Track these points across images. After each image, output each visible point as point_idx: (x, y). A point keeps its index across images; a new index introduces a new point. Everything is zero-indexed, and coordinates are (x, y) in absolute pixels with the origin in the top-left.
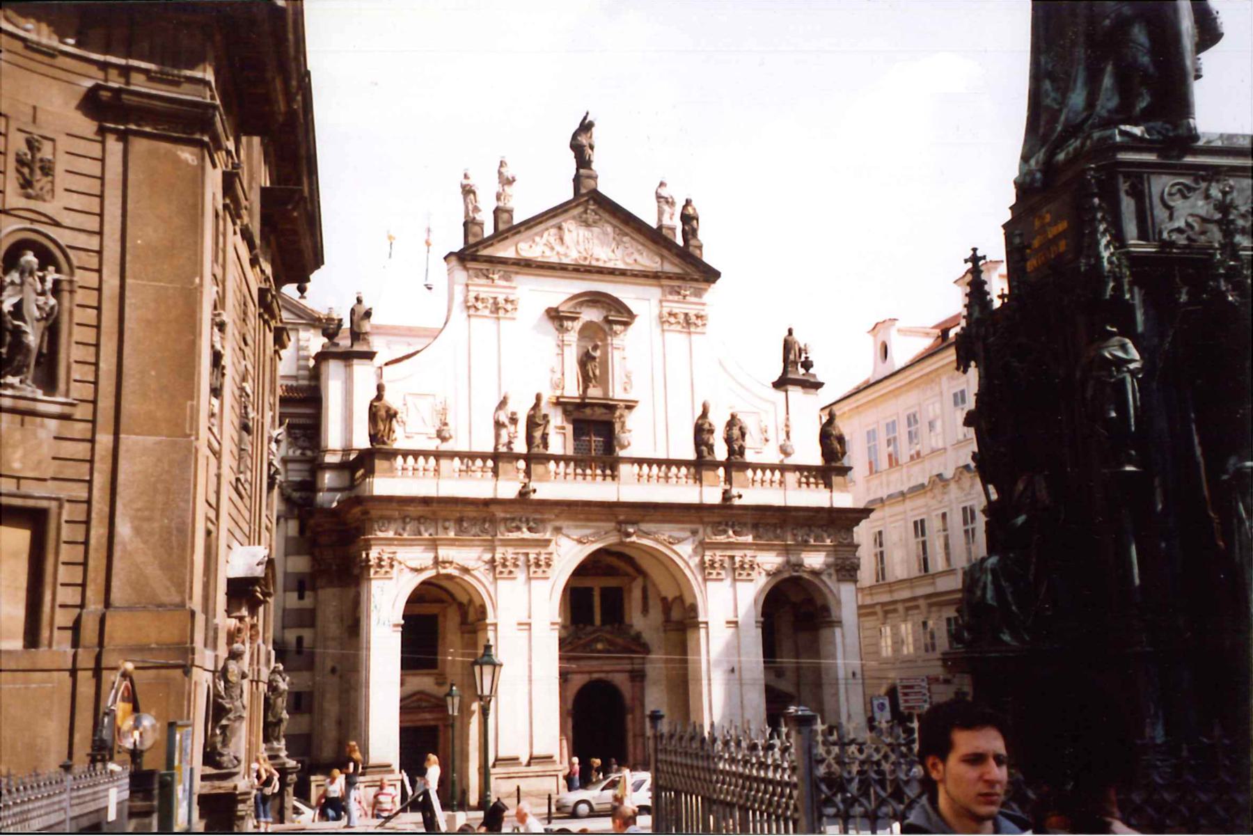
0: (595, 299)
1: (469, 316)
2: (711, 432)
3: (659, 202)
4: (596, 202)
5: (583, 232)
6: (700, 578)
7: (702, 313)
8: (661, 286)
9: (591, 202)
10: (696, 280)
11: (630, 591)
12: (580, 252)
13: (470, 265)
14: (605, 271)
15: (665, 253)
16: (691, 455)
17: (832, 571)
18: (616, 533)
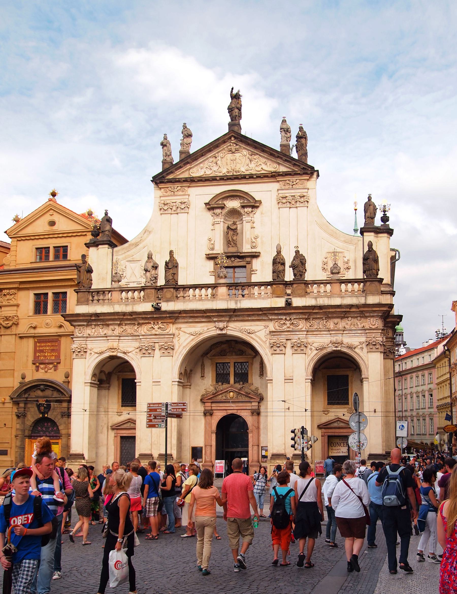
0: (233, 195)
1: (161, 214)
2: (283, 264)
3: (281, 132)
4: (235, 138)
5: (230, 156)
6: (269, 354)
7: (305, 194)
8: (278, 181)
9: (233, 138)
10: (299, 174)
11: (252, 364)
12: (228, 169)
13: (161, 186)
14: (240, 177)
15: (279, 161)
16: (269, 278)
17: (364, 345)
18: (215, 328)
